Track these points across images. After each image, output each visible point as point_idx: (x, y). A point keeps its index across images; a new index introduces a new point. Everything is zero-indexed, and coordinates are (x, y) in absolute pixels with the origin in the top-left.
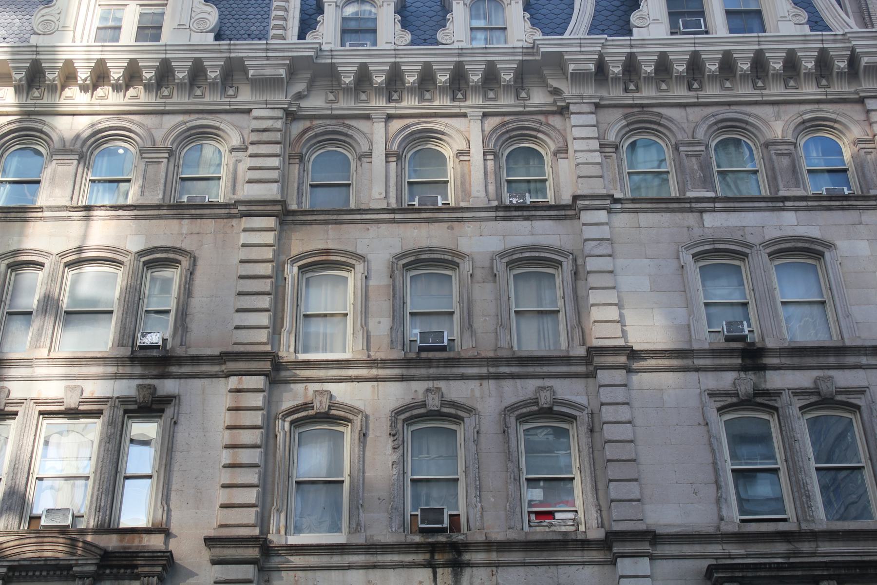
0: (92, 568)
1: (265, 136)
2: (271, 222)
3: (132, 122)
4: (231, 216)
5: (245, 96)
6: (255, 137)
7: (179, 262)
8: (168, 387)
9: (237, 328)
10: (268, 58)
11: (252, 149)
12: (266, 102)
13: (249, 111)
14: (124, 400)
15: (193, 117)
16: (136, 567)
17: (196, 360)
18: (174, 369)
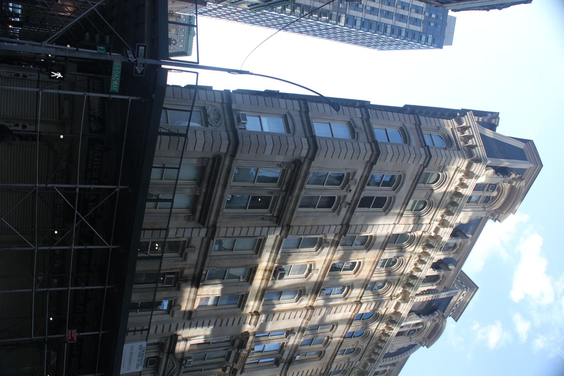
0: (234, 367)
1: (350, 365)
2: (323, 372)
3: (369, 338)
4: (328, 364)
5: (365, 359)
6: (350, 364)
7: (319, 357)
8: (282, 365)
9: (294, 373)
10: (372, 368)
11: (347, 364)
12: (360, 364)
13: (360, 360)
14: (281, 358)
15: (364, 350)
16: (232, 373)
17: (287, 369)
18: (287, 364)
